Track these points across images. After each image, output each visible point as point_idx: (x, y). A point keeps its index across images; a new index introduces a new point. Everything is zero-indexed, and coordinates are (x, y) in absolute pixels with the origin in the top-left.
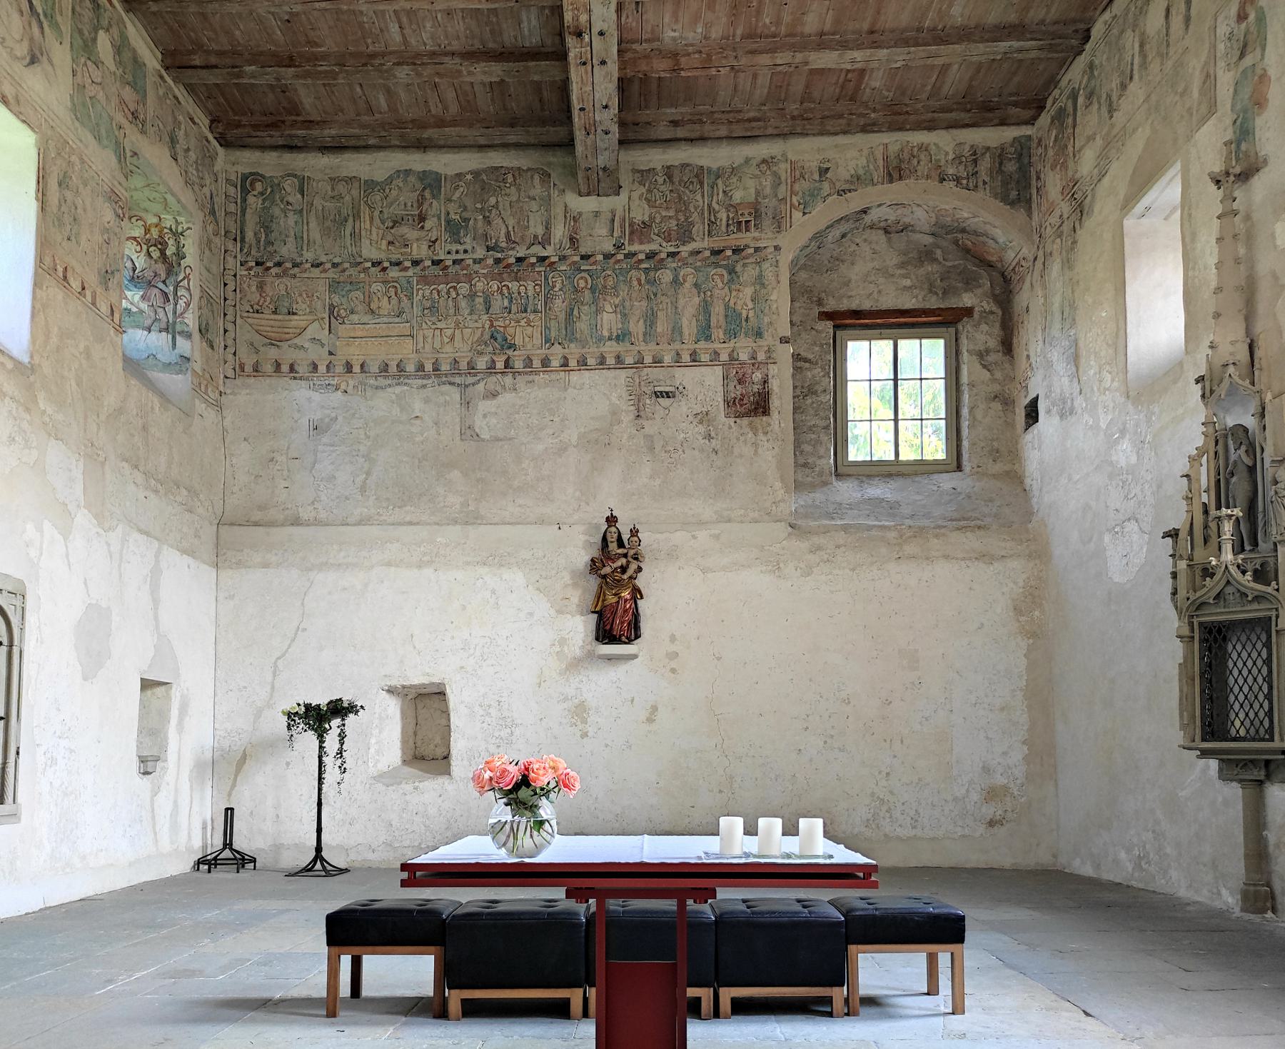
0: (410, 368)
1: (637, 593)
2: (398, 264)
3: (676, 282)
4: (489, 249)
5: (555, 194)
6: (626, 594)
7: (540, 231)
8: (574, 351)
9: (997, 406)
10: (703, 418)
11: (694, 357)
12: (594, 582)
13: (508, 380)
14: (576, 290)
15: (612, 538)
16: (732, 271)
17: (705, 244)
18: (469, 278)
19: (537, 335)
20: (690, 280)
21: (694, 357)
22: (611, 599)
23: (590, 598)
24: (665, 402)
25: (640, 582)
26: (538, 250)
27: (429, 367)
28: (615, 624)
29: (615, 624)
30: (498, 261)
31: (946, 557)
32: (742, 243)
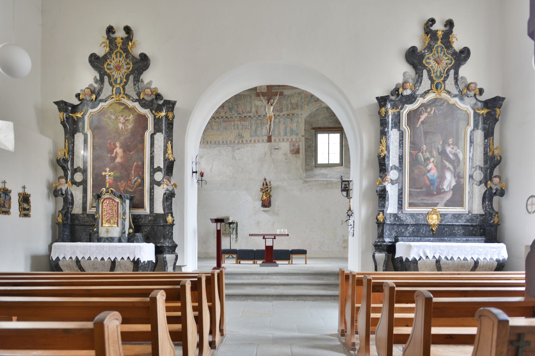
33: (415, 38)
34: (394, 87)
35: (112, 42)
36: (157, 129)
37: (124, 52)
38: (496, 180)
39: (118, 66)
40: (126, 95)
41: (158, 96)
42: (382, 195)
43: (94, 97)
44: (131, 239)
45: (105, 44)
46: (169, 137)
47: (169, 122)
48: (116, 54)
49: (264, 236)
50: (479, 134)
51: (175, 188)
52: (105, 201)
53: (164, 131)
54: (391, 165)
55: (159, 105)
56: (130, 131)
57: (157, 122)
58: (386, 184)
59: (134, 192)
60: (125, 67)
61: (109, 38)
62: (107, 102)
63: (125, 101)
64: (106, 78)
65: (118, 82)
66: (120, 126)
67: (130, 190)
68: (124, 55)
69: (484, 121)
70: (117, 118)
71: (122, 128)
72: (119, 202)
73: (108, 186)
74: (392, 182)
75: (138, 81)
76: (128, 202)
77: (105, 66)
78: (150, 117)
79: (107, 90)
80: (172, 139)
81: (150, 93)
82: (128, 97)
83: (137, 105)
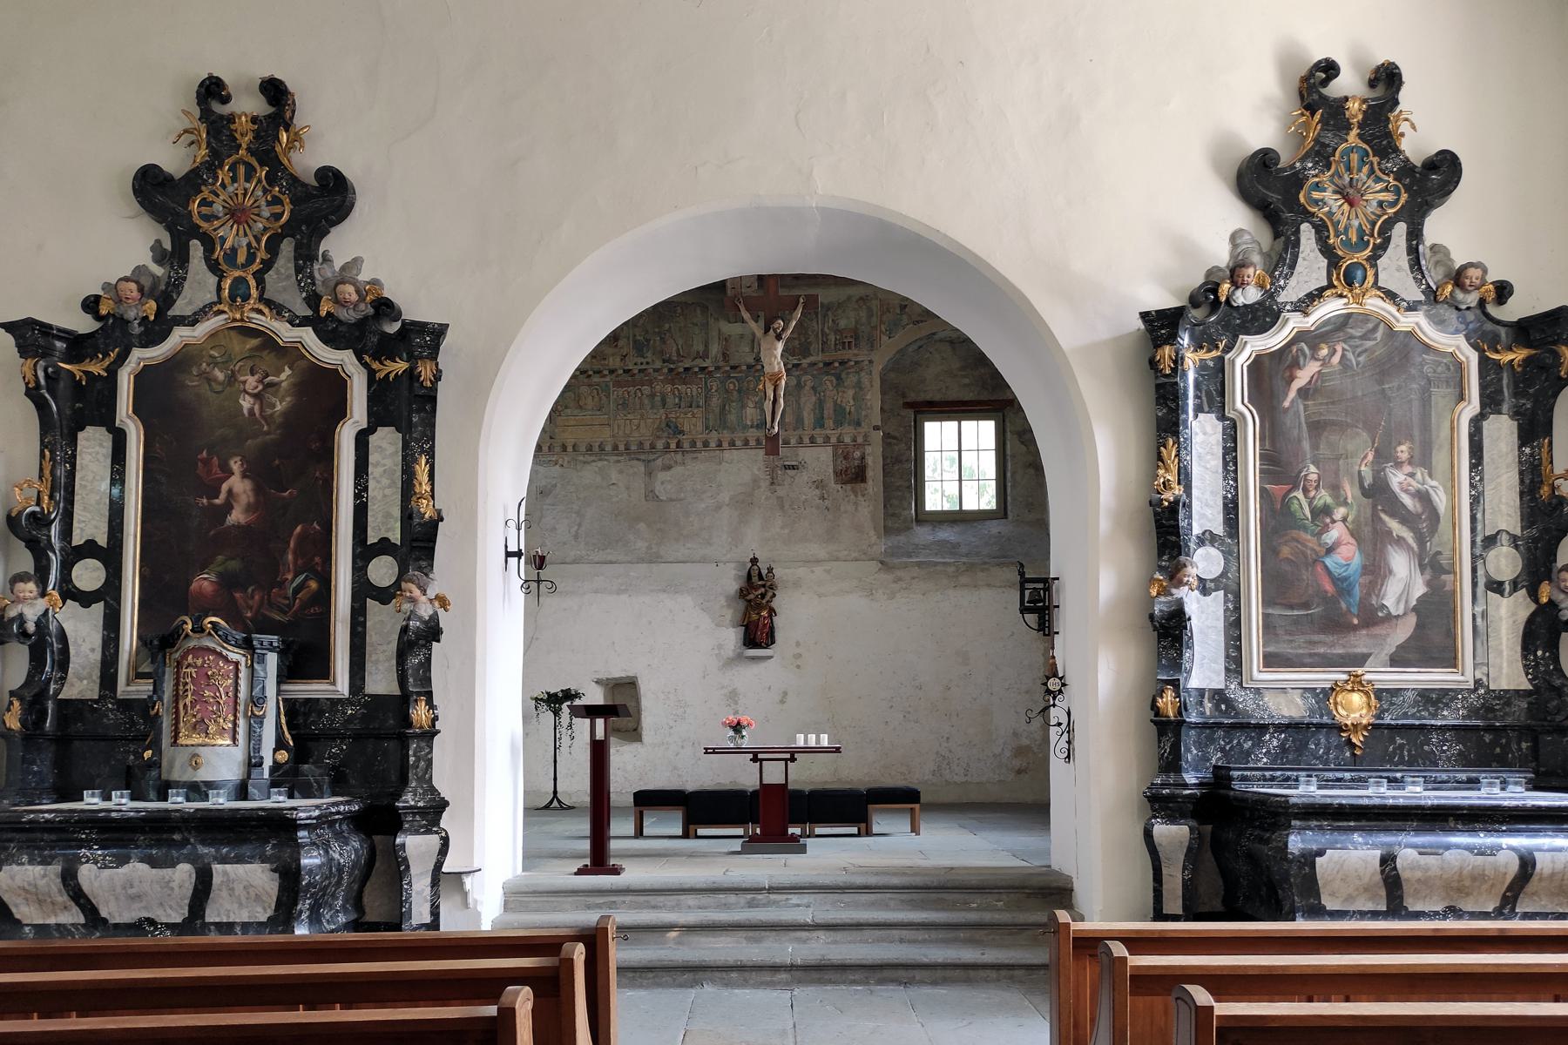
0: (608, 448)
1: (772, 612)
2: (599, 372)
5: (711, 321)
6: (764, 613)
7: (701, 348)
8: (726, 436)
9: (1032, 471)
12: (742, 605)
13: (679, 457)
14: (727, 391)
15: (755, 573)
16: (839, 378)
19: (699, 424)
22: (755, 617)
23: (739, 615)
25: (774, 604)
26: (700, 362)
27: (622, 447)
28: (757, 633)
29: (757, 633)
30: (671, 370)
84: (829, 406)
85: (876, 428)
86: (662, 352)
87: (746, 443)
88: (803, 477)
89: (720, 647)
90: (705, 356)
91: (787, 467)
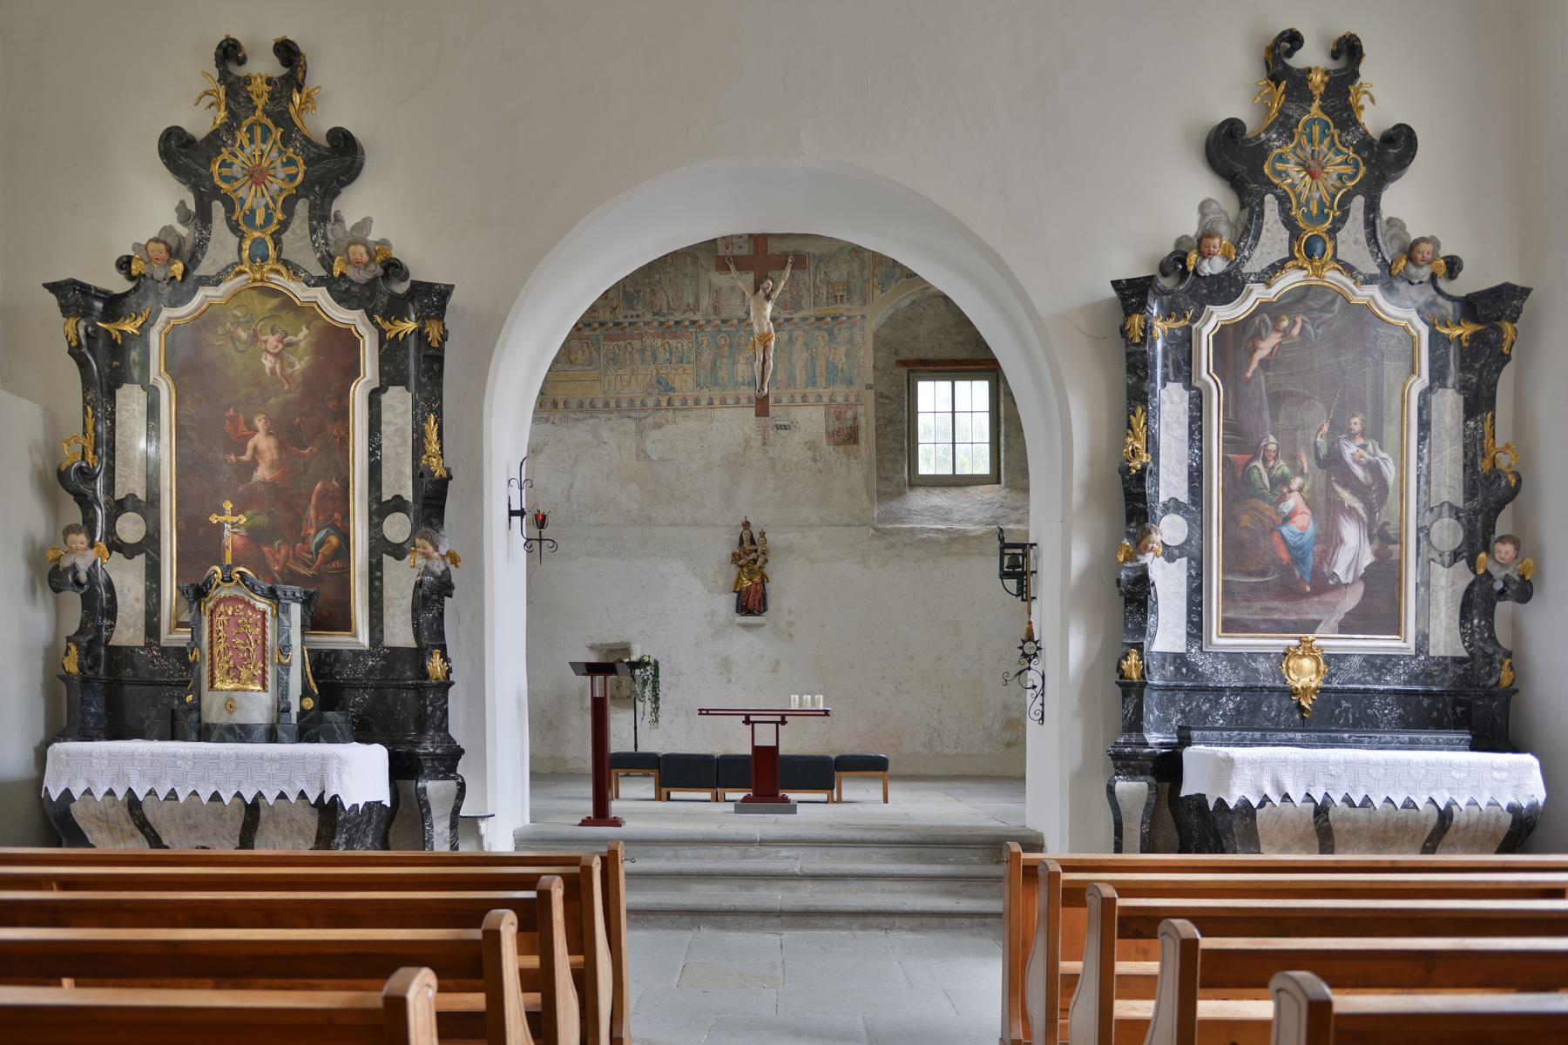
0: (599, 405)
3: (791, 341)
4: (655, 314)
5: (702, 272)
8: (717, 393)
10: (812, 445)
11: (804, 398)
13: (670, 414)
17: (812, 312)
18: (640, 336)
20: (801, 340)
21: (804, 398)
24: (783, 433)
25: (767, 570)
26: (690, 316)
27: (613, 404)
30: (661, 324)
31: (981, 554)
32: (837, 312)
33: (1234, 95)
34: (1170, 248)
35: (235, 90)
36: (391, 375)
37: (277, 125)
38: (1505, 551)
39: (259, 170)
40: (286, 263)
41: (393, 268)
42: (1136, 596)
43: (178, 268)
44: (309, 730)
45: (213, 99)
46: (430, 401)
47: (430, 352)
48: (250, 129)
49: (747, 717)
50: (1448, 403)
51: (452, 567)
52: (222, 608)
53: (412, 382)
54: (1163, 498)
55: (394, 296)
56: (299, 379)
57: (390, 351)
58: (1148, 559)
59: (317, 579)
60: (281, 173)
61: (224, 77)
62: (224, 287)
63: (283, 282)
64: (218, 209)
65: (259, 220)
66: (268, 362)
67: (303, 571)
68: (277, 133)
69: (1463, 360)
70: (255, 337)
71: (273, 371)
72: (269, 610)
73: (228, 561)
74: (1169, 554)
75: (324, 219)
76: (296, 610)
77: (215, 168)
78: (367, 337)
79: (222, 247)
80: (441, 406)
81: (365, 258)
82: (293, 269)
83: (321, 295)
84: (821, 362)
85: (869, 387)
86: (652, 304)
87: (738, 401)
88: (796, 439)
89: (713, 613)
90: (695, 309)
91: (778, 427)
